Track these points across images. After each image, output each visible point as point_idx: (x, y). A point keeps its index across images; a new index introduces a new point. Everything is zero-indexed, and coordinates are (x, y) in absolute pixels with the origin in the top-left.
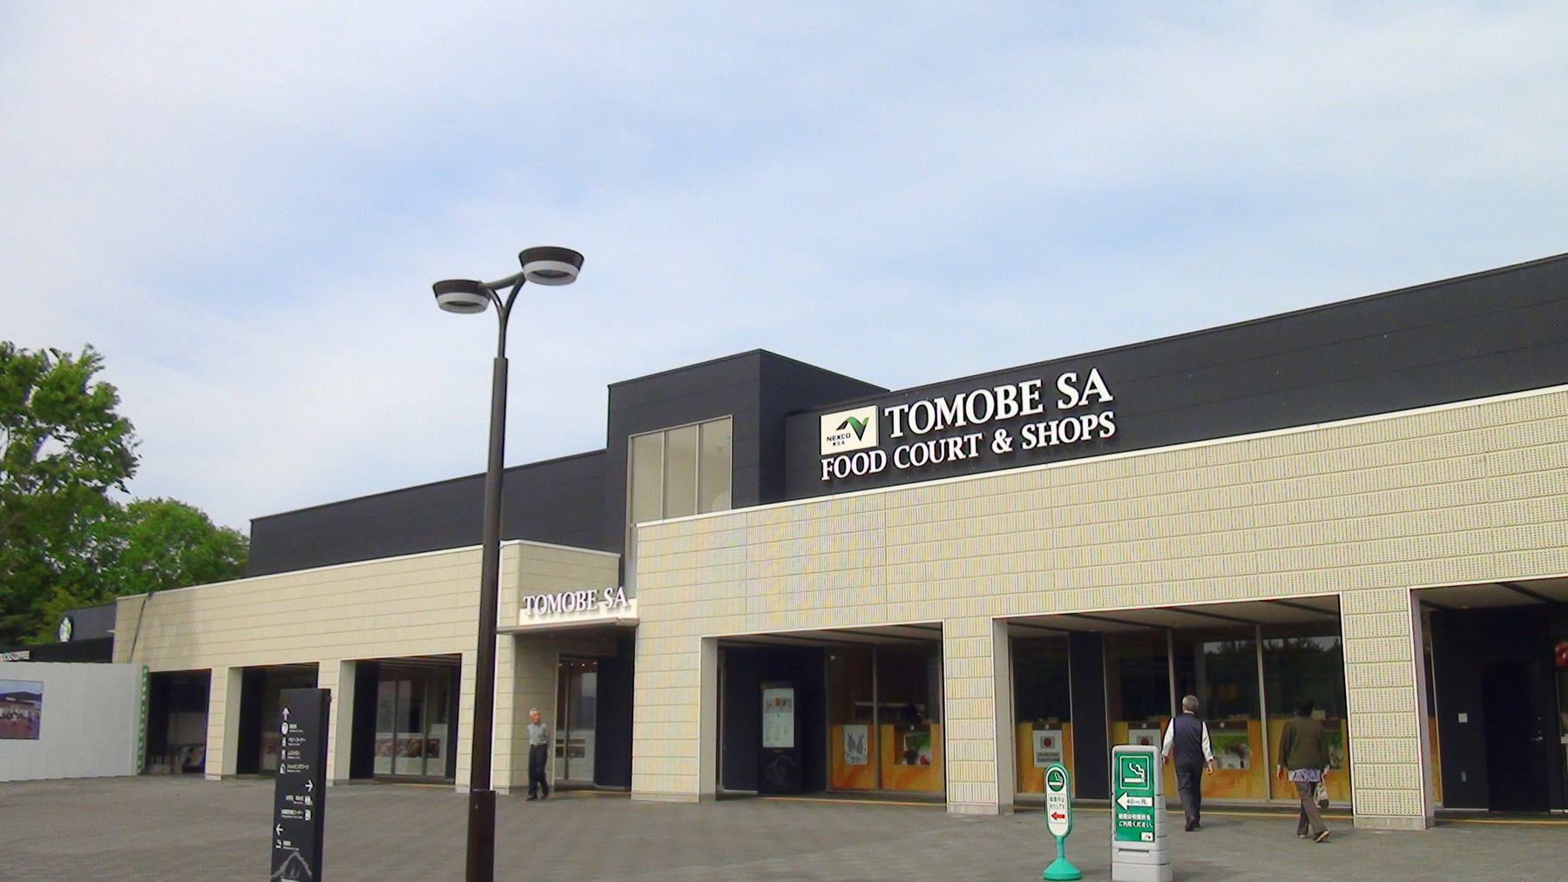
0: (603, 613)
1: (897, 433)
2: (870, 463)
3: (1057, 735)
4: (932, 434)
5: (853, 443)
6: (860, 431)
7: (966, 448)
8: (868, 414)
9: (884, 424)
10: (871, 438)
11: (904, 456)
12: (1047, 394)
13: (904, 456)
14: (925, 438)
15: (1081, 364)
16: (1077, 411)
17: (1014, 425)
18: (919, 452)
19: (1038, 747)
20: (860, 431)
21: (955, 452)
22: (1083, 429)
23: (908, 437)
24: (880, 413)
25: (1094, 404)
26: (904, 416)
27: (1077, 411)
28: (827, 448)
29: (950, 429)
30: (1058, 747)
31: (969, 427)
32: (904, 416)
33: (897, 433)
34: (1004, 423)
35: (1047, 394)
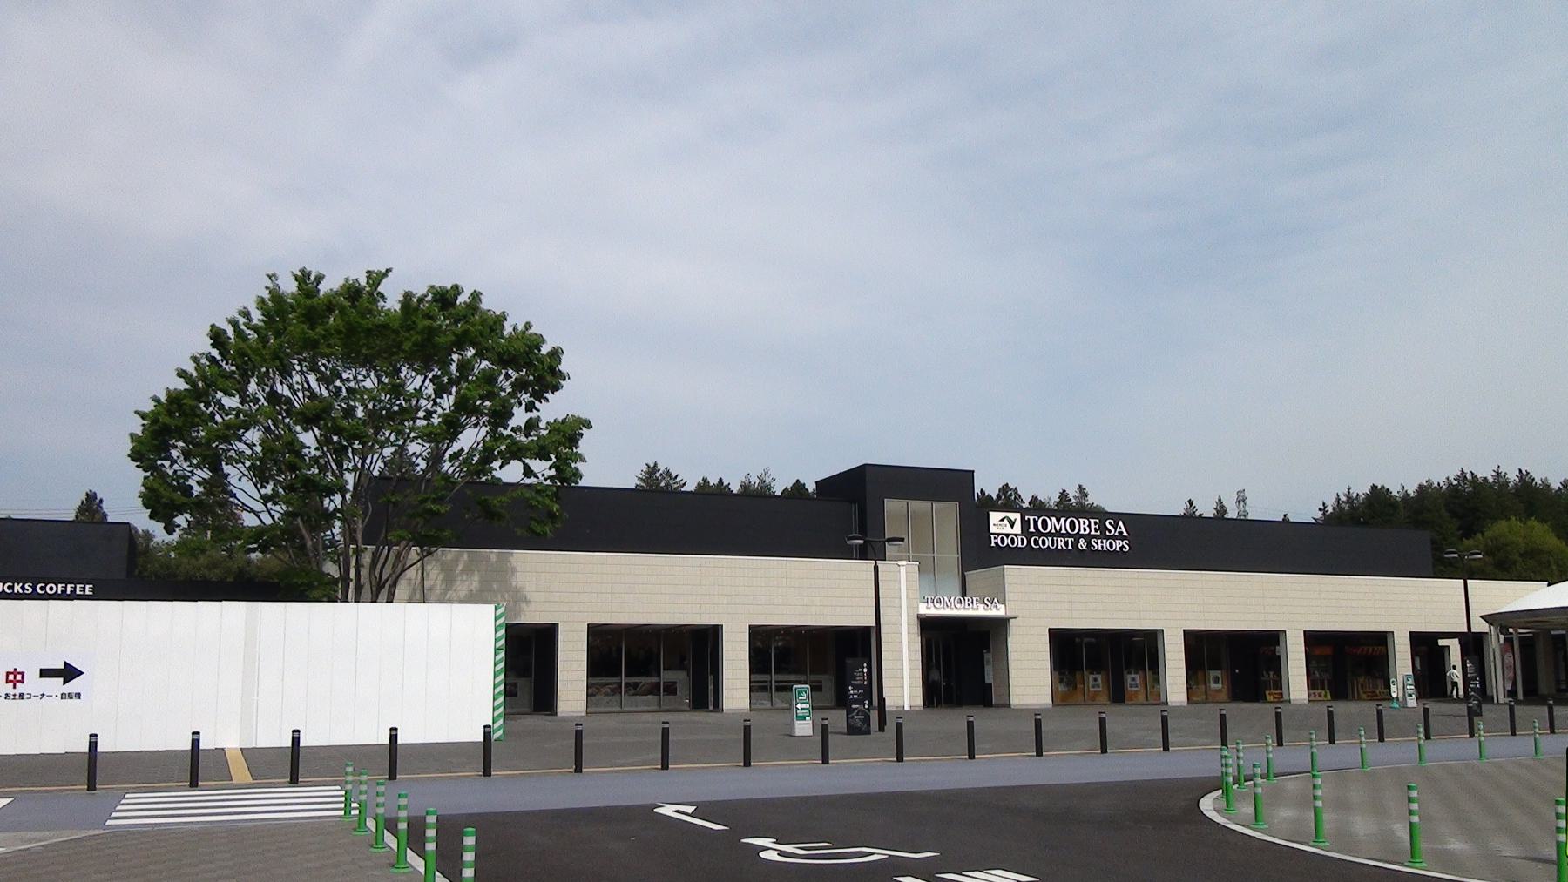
0: (981, 611)
2: (1018, 542)
3: (1099, 677)
5: (1008, 530)
6: (1012, 524)
7: (1066, 544)
9: (1025, 524)
10: (1017, 529)
11: (1036, 542)
13: (1036, 542)
14: (1047, 535)
15: (1117, 517)
17: (1088, 538)
20: (1012, 524)
21: (1061, 545)
22: (1117, 545)
26: (1036, 522)
28: (993, 529)
29: (1059, 534)
31: (1070, 536)
32: (1036, 522)
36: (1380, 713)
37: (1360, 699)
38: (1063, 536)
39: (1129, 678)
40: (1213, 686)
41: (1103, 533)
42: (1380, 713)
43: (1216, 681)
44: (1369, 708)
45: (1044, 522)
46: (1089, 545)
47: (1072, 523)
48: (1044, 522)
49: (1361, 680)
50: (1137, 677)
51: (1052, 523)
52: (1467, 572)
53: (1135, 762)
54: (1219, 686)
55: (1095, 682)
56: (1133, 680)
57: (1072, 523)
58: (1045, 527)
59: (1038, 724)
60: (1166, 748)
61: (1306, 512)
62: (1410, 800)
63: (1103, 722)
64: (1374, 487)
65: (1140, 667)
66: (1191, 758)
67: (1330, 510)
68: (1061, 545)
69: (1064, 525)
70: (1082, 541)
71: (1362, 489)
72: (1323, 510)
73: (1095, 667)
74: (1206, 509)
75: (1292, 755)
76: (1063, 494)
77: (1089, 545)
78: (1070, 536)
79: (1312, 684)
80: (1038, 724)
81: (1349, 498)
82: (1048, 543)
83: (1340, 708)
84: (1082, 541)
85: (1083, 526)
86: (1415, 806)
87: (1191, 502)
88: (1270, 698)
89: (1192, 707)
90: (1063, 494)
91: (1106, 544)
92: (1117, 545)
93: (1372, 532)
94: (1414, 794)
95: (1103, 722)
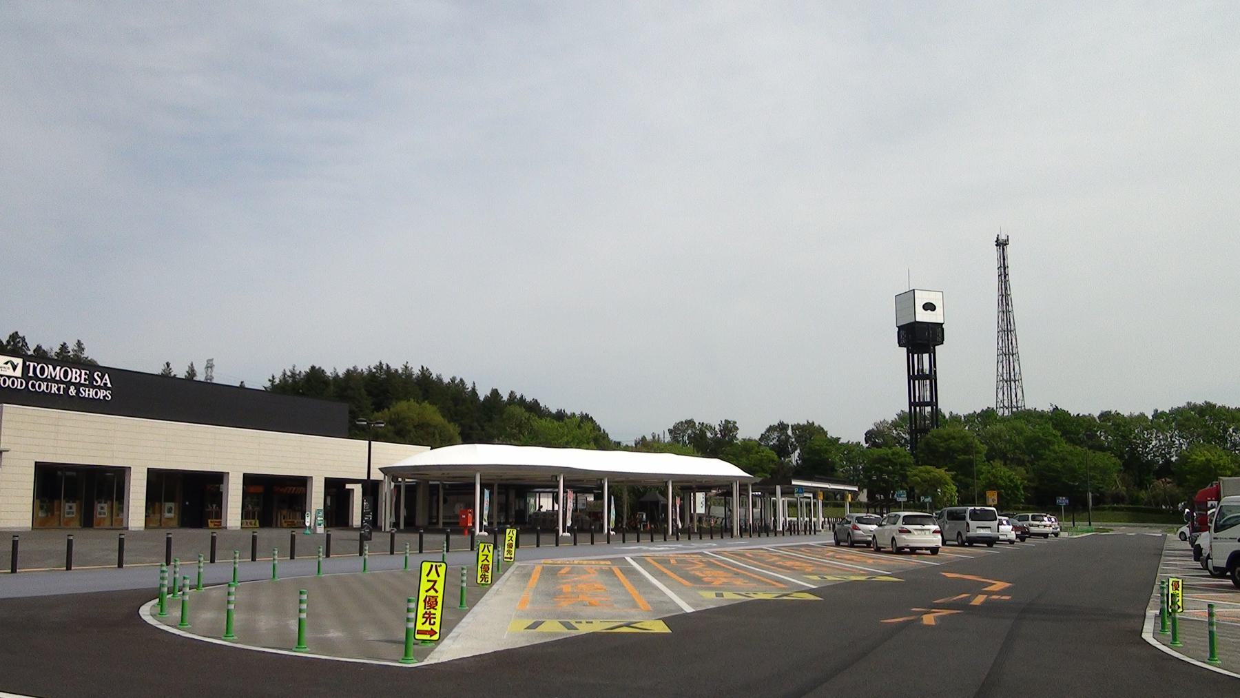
1: (31, 374)
3: (74, 505)
4: (46, 380)
7: (59, 389)
8: (18, 361)
9: (25, 368)
11: (33, 386)
12: (91, 378)
13: (33, 386)
15: (104, 370)
16: (100, 387)
17: (78, 386)
18: (40, 386)
19: (67, 509)
21: (54, 390)
22: (101, 394)
23: (36, 378)
24: (24, 363)
25: (105, 387)
26: (35, 368)
27: (100, 387)
29: (53, 380)
30: (74, 510)
31: (63, 383)
32: (35, 368)
33: (31, 374)
34: (73, 384)
35: (91, 378)
36: (293, 538)
37: (282, 527)
38: (57, 382)
39: (98, 507)
40: (167, 515)
41: (91, 383)
42: (293, 538)
43: (170, 511)
44: (285, 534)
45: (42, 368)
46: (78, 392)
47: (66, 373)
48: (42, 368)
49: (284, 512)
50: (105, 506)
51: (49, 370)
52: (372, 435)
53: (94, 577)
54: (171, 515)
55: (70, 510)
56: (102, 509)
57: (66, 373)
58: (42, 374)
59: (15, 544)
60: (120, 565)
61: (258, 381)
62: (301, 601)
63: (70, 543)
64: (313, 367)
65: (109, 498)
66: (141, 573)
67: (277, 381)
68: (54, 390)
69: (59, 373)
70: (72, 388)
71: (303, 368)
72: (272, 381)
73: (70, 497)
74: (180, 372)
75: (220, 570)
76: (64, 347)
77: (78, 392)
78: (63, 383)
79: (246, 515)
80: (15, 544)
81: (293, 374)
82: (44, 387)
83: (264, 534)
84: (72, 388)
85: (75, 375)
86: (304, 606)
87: (168, 364)
88: (211, 525)
89: (148, 532)
90: (64, 347)
91: (92, 393)
92: (101, 394)
93: (310, 401)
94: (305, 597)
95: (70, 543)
